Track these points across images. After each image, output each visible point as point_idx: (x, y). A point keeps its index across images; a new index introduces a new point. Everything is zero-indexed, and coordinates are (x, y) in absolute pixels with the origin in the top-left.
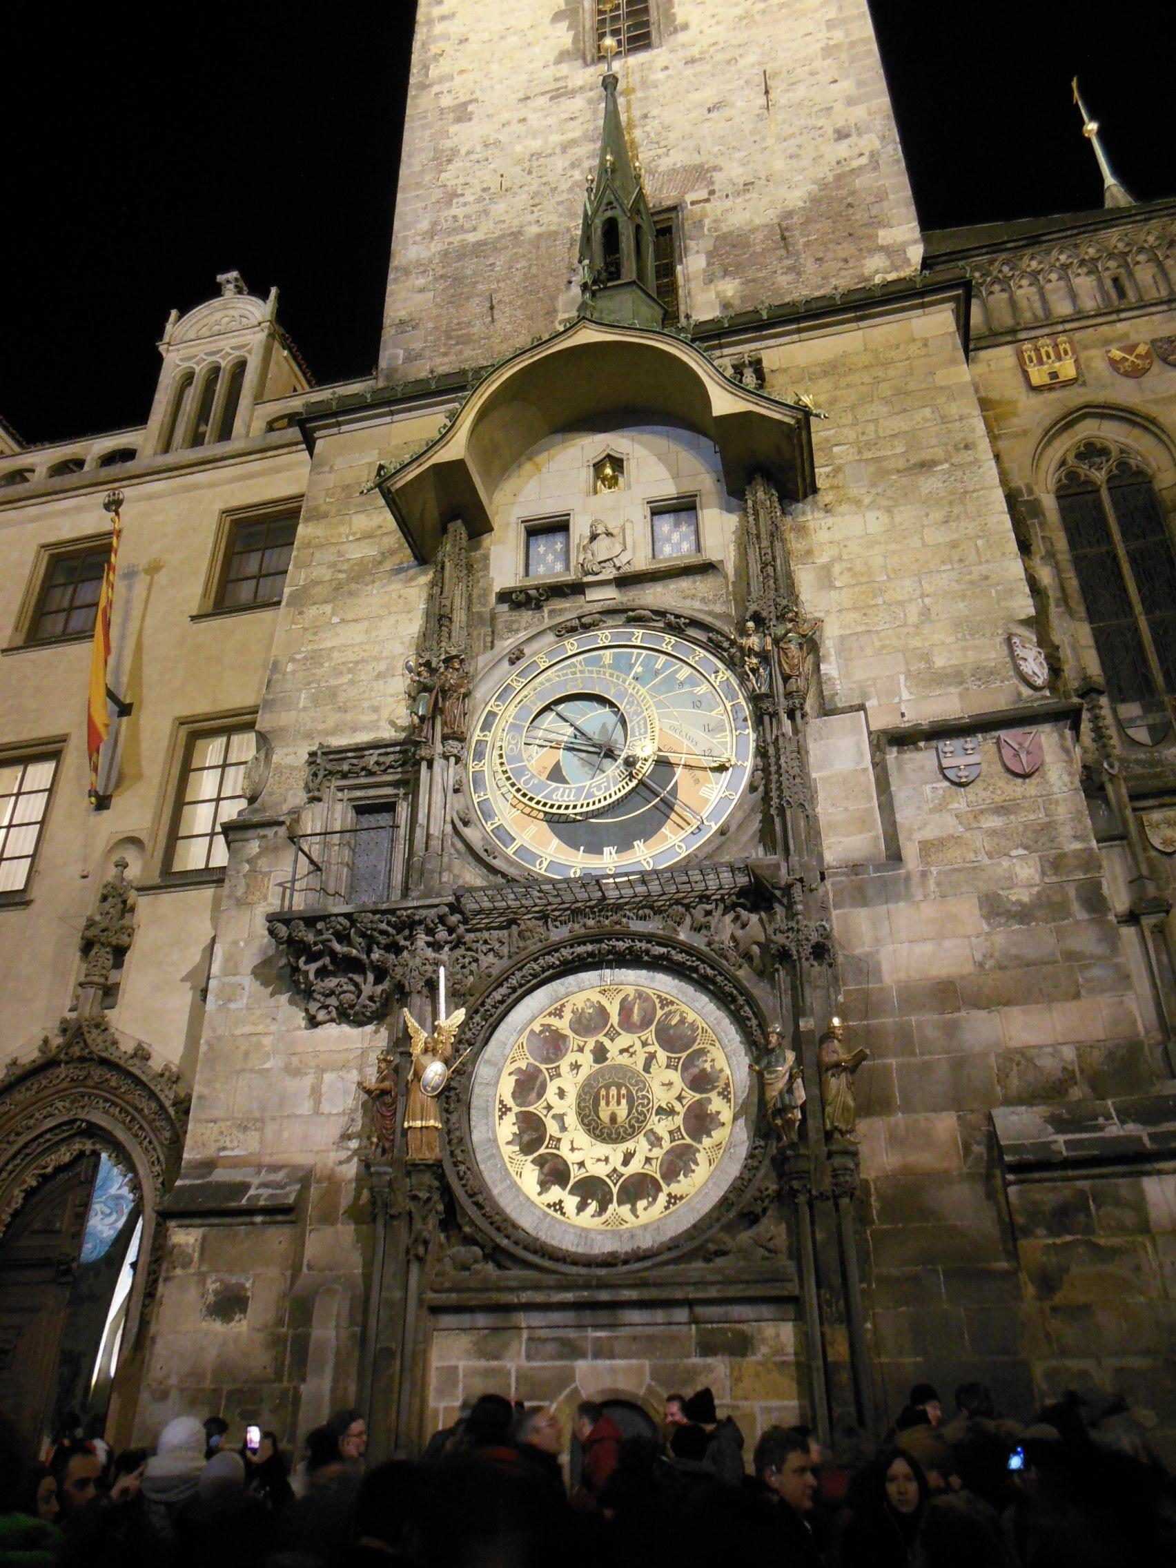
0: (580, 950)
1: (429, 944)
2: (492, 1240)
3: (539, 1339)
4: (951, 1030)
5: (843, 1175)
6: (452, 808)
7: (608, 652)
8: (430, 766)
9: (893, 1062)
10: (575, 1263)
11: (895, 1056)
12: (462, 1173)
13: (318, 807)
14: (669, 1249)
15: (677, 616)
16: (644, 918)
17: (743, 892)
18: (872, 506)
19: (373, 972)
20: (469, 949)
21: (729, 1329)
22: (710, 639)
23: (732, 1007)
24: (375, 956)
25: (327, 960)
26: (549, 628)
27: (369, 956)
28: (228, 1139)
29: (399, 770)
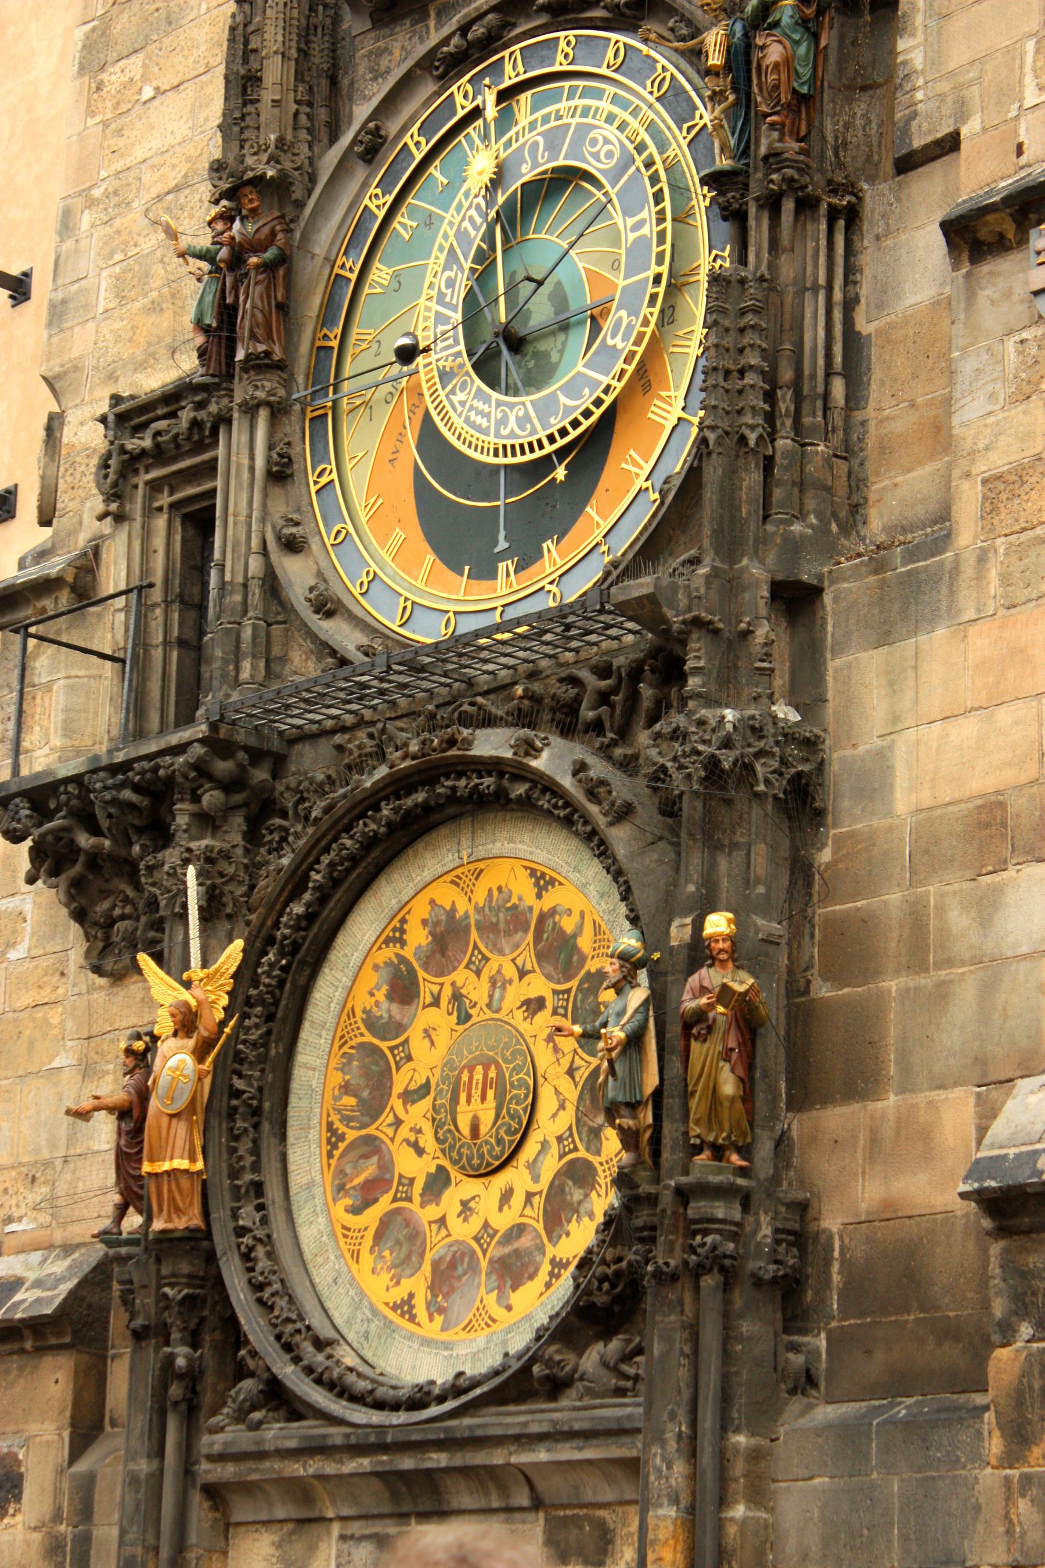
0: (409, 802)
2: (268, 1369)
3: (352, 1537)
5: (706, 1233)
6: (263, 520)
7: (522, 97)
9: (892, 985)
10: (380, 1405)
11: (897, 972)
12: (243, 1248)
13: (122, 536)
14: (496, 1373)
17: (655, 653)
21: (587, 1517)
24: (136, 849)
26: (418, 64)
28: (14, 1202)
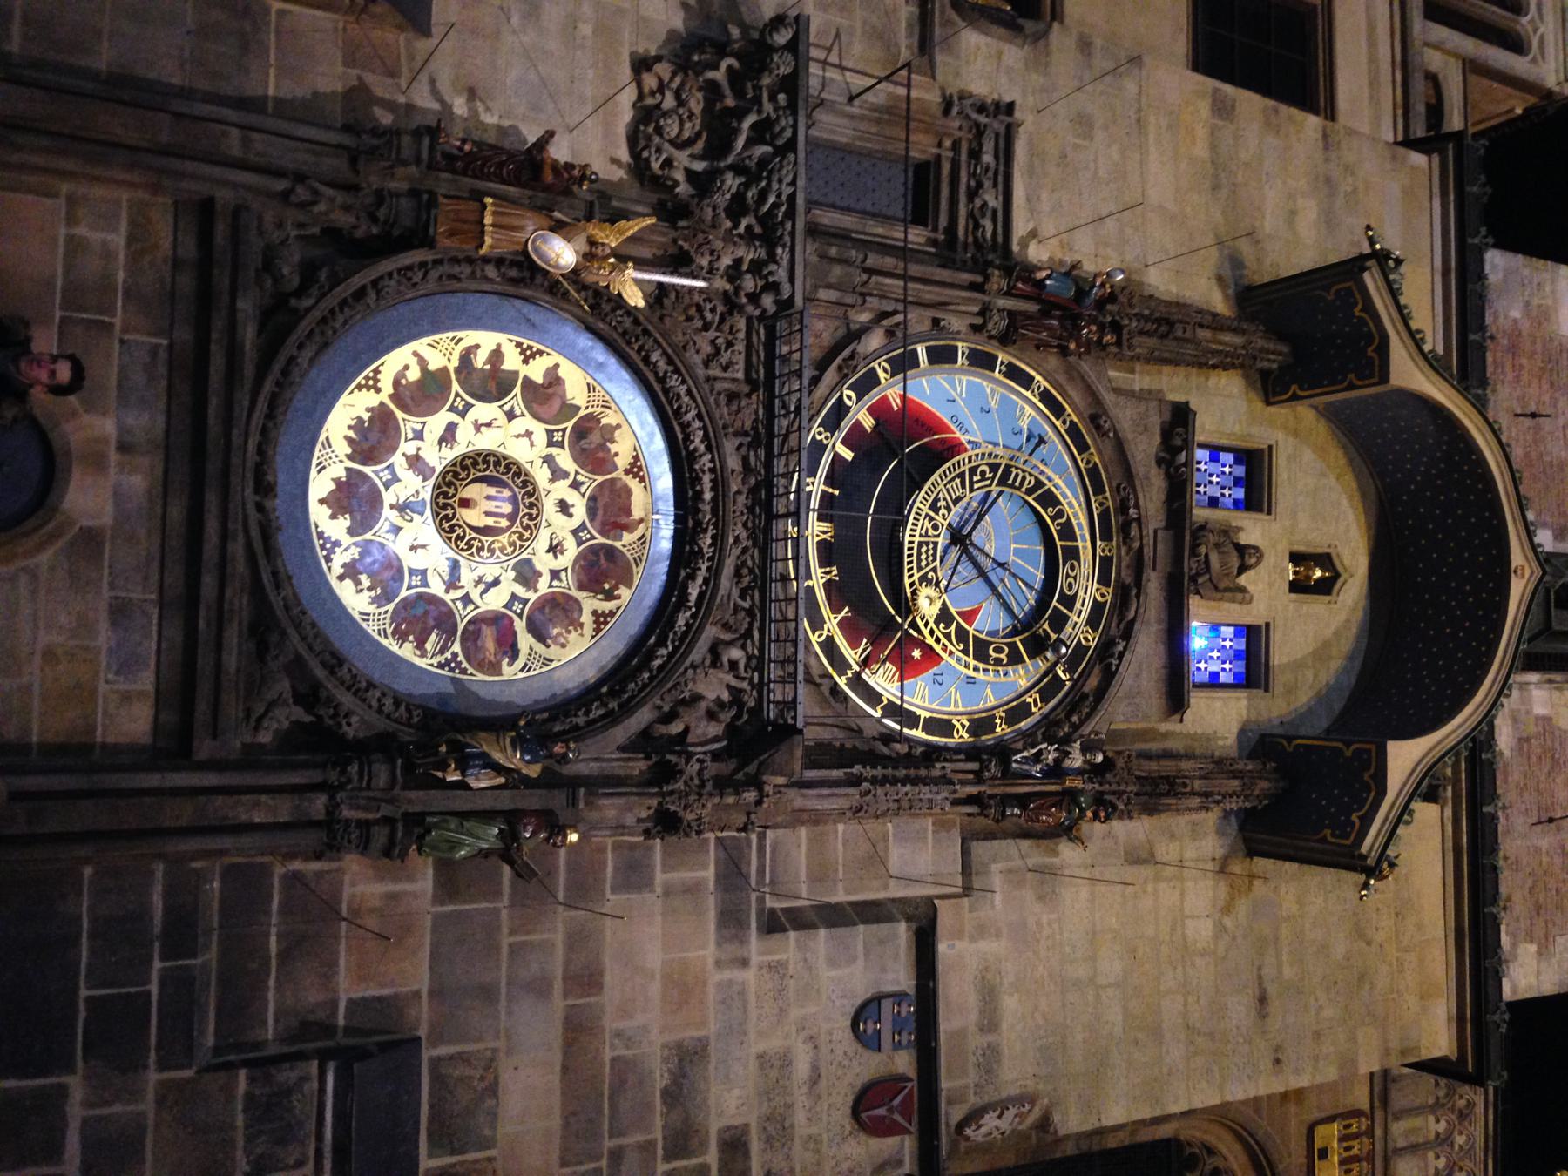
1: (738, 262)
2: (308, 310)
4: (540, 988)
8: (973, 287)
12: (410, 274)
14: (275, 574)
15: (1121, 655)
16: (738, 574)
18: (1220, 929)
19: (705, 171)
20: (722, 320)
22: (1084, 697)
23: (605, 689)
25: (730, 102)
27: (731, 167)
29: (970, 239)
